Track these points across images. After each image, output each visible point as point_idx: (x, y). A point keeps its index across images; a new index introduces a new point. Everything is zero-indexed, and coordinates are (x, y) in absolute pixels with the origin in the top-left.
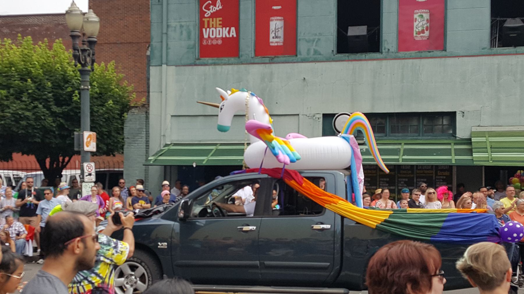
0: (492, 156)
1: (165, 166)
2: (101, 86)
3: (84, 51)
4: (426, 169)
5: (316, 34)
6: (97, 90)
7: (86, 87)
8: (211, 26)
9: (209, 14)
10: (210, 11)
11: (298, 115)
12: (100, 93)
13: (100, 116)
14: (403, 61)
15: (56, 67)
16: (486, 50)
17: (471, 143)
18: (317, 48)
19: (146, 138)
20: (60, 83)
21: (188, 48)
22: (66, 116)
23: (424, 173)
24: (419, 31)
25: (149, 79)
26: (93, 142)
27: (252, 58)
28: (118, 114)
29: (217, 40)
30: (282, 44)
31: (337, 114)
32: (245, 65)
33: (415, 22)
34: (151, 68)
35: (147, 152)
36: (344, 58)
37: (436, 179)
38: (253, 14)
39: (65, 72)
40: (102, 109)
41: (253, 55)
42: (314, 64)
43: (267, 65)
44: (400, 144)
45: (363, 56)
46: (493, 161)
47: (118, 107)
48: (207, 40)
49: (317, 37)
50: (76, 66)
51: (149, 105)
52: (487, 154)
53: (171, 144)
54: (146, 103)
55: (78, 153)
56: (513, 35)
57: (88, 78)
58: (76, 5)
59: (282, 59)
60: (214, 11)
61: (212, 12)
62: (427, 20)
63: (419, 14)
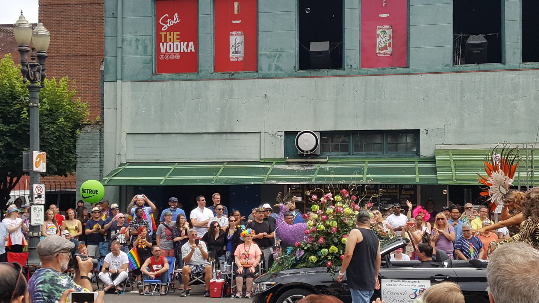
0: (456, 174)
1: (121, 187)
2: (51, 102)
3: (33, 66)
4: (390, 189)
5: (277, 50)
6: (47, 106)
7: (36, 105)
8: (168, 40)
9: (166, 27)
10: (167, 25)
11: (260, 132)
12: (51, 110)
13: (50, 134)
14: (366, 77)
15: (4, 83)
16: (448, 67)
17: (435, 161)
18: (278, 64)
19: (100, 158)
20: (7, 100)
21: (144, 64)
22: (14, 134)
23: (389, 193)
24: (381, 48)
25: (103, 95)
26: (43, 162)
27: (211, 73)
28: (70, 132)
29: (175, 55)
30: (242, 59)
31: (300, 132)
32: (203, 81)
33: (378, 38)
34: (105, 83)
35: (101, 172)
36: (306, 74)
37: (400, 198)
38: (212, 29)
39: (13, 87)
40: (53, 127)
41: (212, 71)
42: (276, 79)
43: (227, 81)
44: (364, 162)
45: (326, 72)
46: (457, 180)
47: (70, 124)
48: (165, 55)
49: (278, 53)
50: (24, 82)
51: (103, 122)
52: (451, 172)
53: (127, 163)
54: (100, 121)
55: (28, 173)
56: (476, 52)
57: (38, 95)
58: (24, 18)
59: (242, 74)
60: (171, 24)
61: (169, 26)
62: (390, 36)
63: (382, 30)
